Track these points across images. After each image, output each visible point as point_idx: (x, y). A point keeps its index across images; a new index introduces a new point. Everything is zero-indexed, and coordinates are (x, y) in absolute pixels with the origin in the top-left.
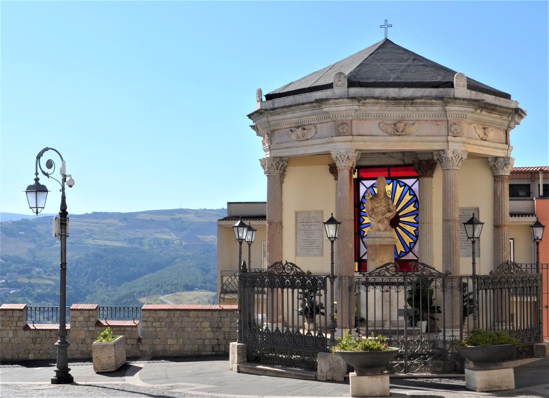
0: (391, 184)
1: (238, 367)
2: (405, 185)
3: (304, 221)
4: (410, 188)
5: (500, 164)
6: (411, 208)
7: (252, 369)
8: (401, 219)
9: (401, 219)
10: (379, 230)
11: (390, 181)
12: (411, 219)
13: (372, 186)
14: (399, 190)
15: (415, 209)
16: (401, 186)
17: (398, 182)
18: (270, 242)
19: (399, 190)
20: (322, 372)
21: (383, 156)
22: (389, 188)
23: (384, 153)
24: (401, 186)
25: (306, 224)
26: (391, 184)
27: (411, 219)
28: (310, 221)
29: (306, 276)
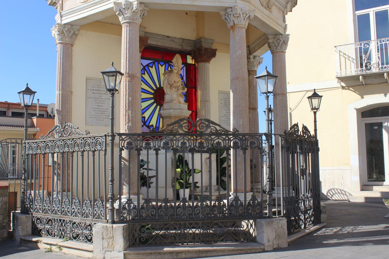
0: (164, 66)
1: (124, 254)
3: (95, 89)
5: (256, 62)
7: (160, 253)
10: (180, 103)
11: (163, 63)
13: (148, 65)
18: (132, 99)
20: (269, 241)
21: (167, 39)
23: (168, 37)
25: (96, 92)
26: (164, 66)
28: (101, 89)
29: (230, 135)
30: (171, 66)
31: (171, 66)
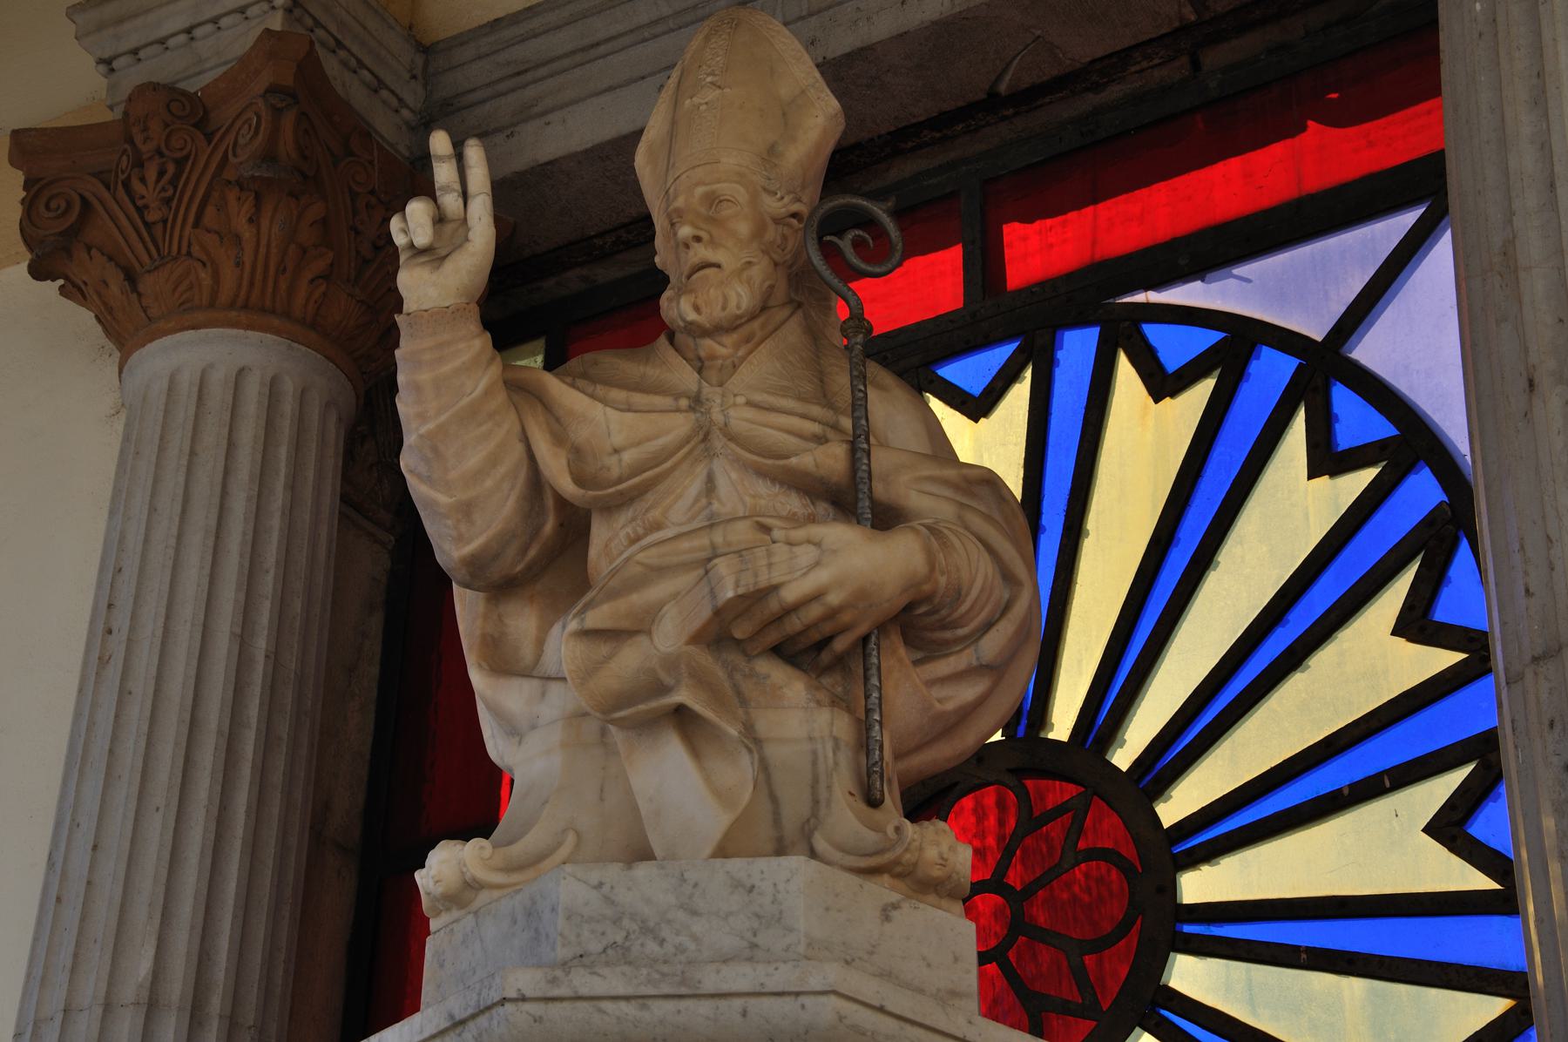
0: (1019, 396)
2: (1239, 341)
4: (1324, 367)
6: (1373, 659)
8: (1199, 886)
9: (1199, 886)
12: (1385, 848)
14: (1146, 438)
15: (1444, 659)
16: (1162, 385)
17: (1124, 334)
19: (1146, 438)
22: (993, 443)
24: (1162, 385)
26: (1019, 396)
27: (1385, 848)
30: (1153, 332)
31: (1153, 332)
